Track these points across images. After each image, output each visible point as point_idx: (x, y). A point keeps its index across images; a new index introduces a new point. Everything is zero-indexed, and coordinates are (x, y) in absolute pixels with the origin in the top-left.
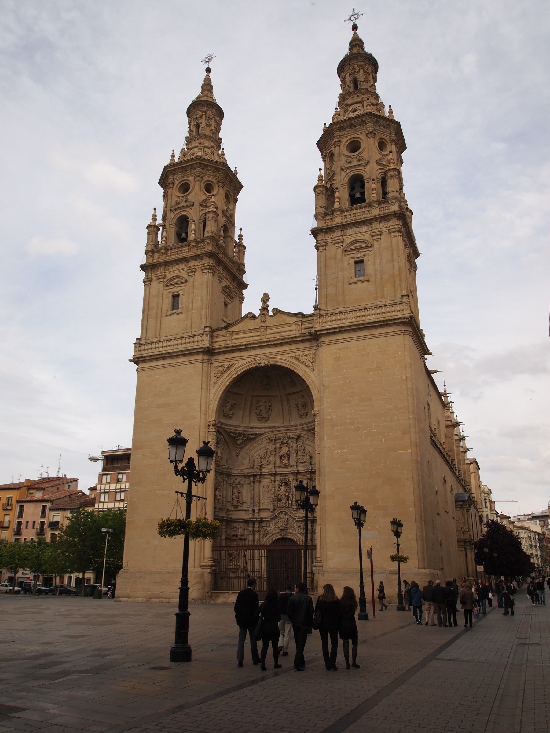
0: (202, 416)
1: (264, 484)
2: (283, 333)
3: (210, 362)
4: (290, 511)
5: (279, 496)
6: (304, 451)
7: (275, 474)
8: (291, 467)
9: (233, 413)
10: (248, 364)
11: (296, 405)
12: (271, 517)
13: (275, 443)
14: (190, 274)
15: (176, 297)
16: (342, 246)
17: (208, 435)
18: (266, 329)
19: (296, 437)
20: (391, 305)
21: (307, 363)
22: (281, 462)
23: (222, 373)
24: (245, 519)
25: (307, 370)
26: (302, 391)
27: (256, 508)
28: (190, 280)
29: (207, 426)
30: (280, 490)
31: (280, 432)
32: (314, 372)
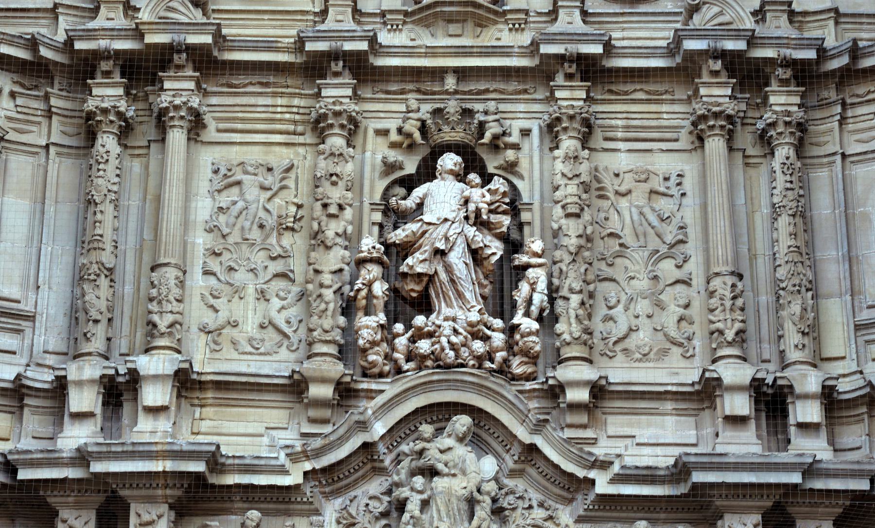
1: (235, 154)
5: (415, 262)
8: (517, 28)
12: (319, 453)
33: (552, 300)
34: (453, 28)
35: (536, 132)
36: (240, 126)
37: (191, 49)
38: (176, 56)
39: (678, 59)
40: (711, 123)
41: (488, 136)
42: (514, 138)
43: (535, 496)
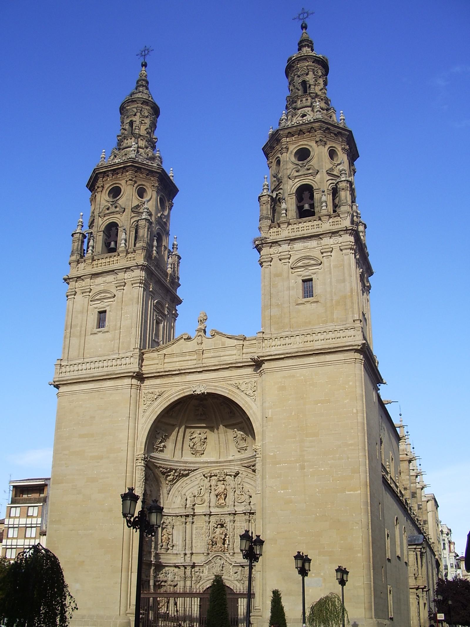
1: (198, 525)
2: (222, 358)
3: (139, 388)
4: (226, 555)
6: (242, 489)
10: (182, 391)
11: (235, 437)
12: (205, 562)
13: (210, 480)
14: (118, 288)
15: (102, 313)
18: (203, 352)
20: (342, 330)
23: (153, 401)
24: (175, 564)
25: (248, 399)
26: (242, 422)
27: (188, 552)
28: (119, 294)
30: (215, 533)
31: (216, 468)
32: (256, 403)
33: (229, 542)
37: (191, 515)
43: (228, 565)
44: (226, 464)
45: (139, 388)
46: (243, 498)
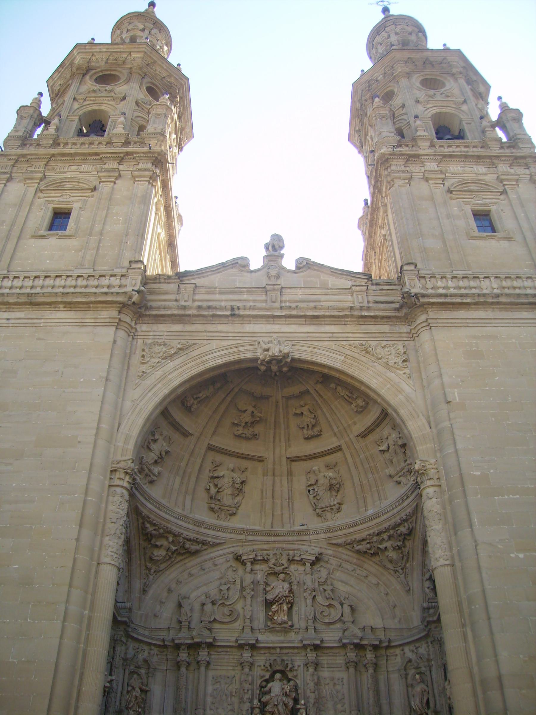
0: (101, 443)
7: (253, 647)
9: (159, 473)
10: (235, 350)
11: (309, 486)
16: (444, 184)
17: (108, 495)
19: (314, 558)
21: (394, 362)
22: (269, 618)
26: (338, 449)
29: (109, 472)
30: (269, 692)
31: (265, 546)
34: (279, 634)
35: (302, 666)
36: (220, 664)
38: (203, 645)
39: (341, 644)
40: (351, 664)
41: (288, 669)
42: (296, 668)
44: (291, 538)
45: (132, 334)
46: (335, 614)
